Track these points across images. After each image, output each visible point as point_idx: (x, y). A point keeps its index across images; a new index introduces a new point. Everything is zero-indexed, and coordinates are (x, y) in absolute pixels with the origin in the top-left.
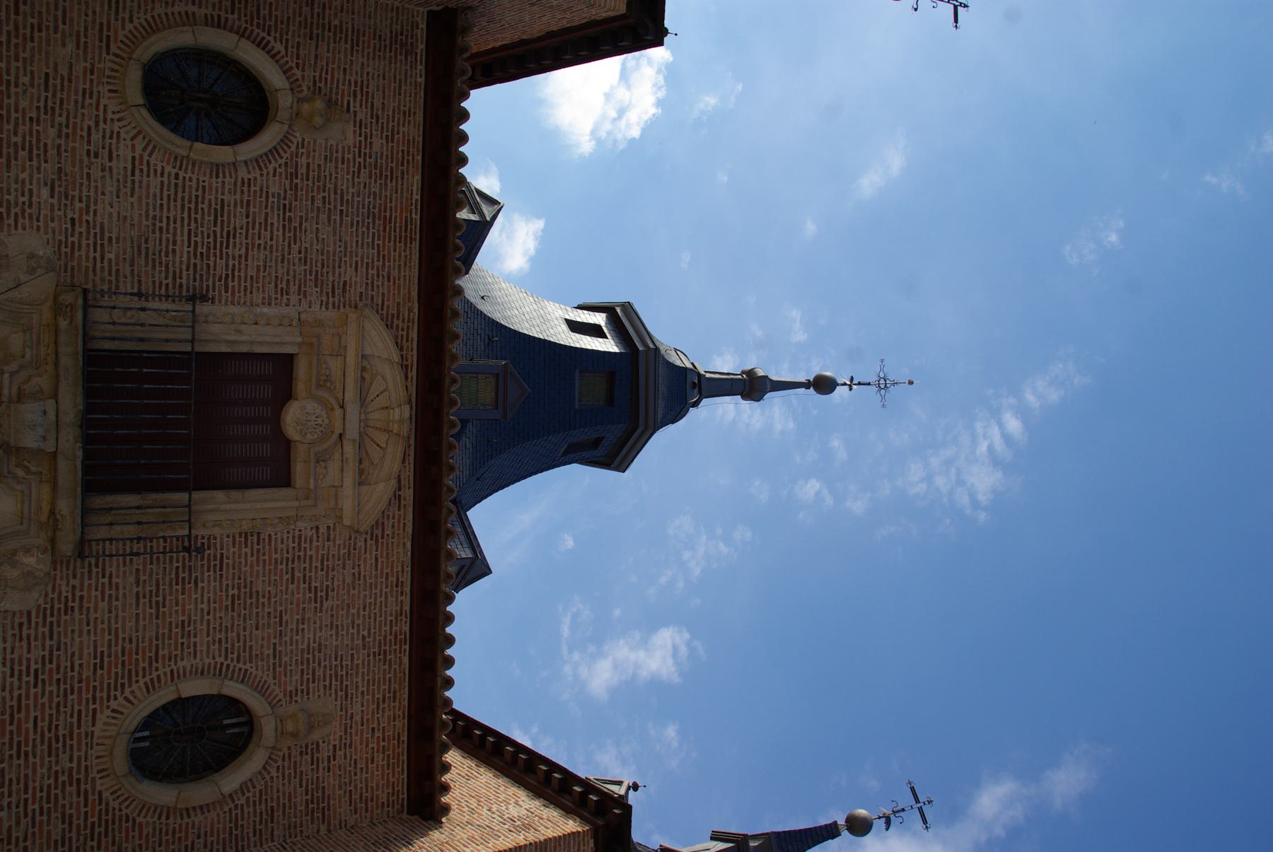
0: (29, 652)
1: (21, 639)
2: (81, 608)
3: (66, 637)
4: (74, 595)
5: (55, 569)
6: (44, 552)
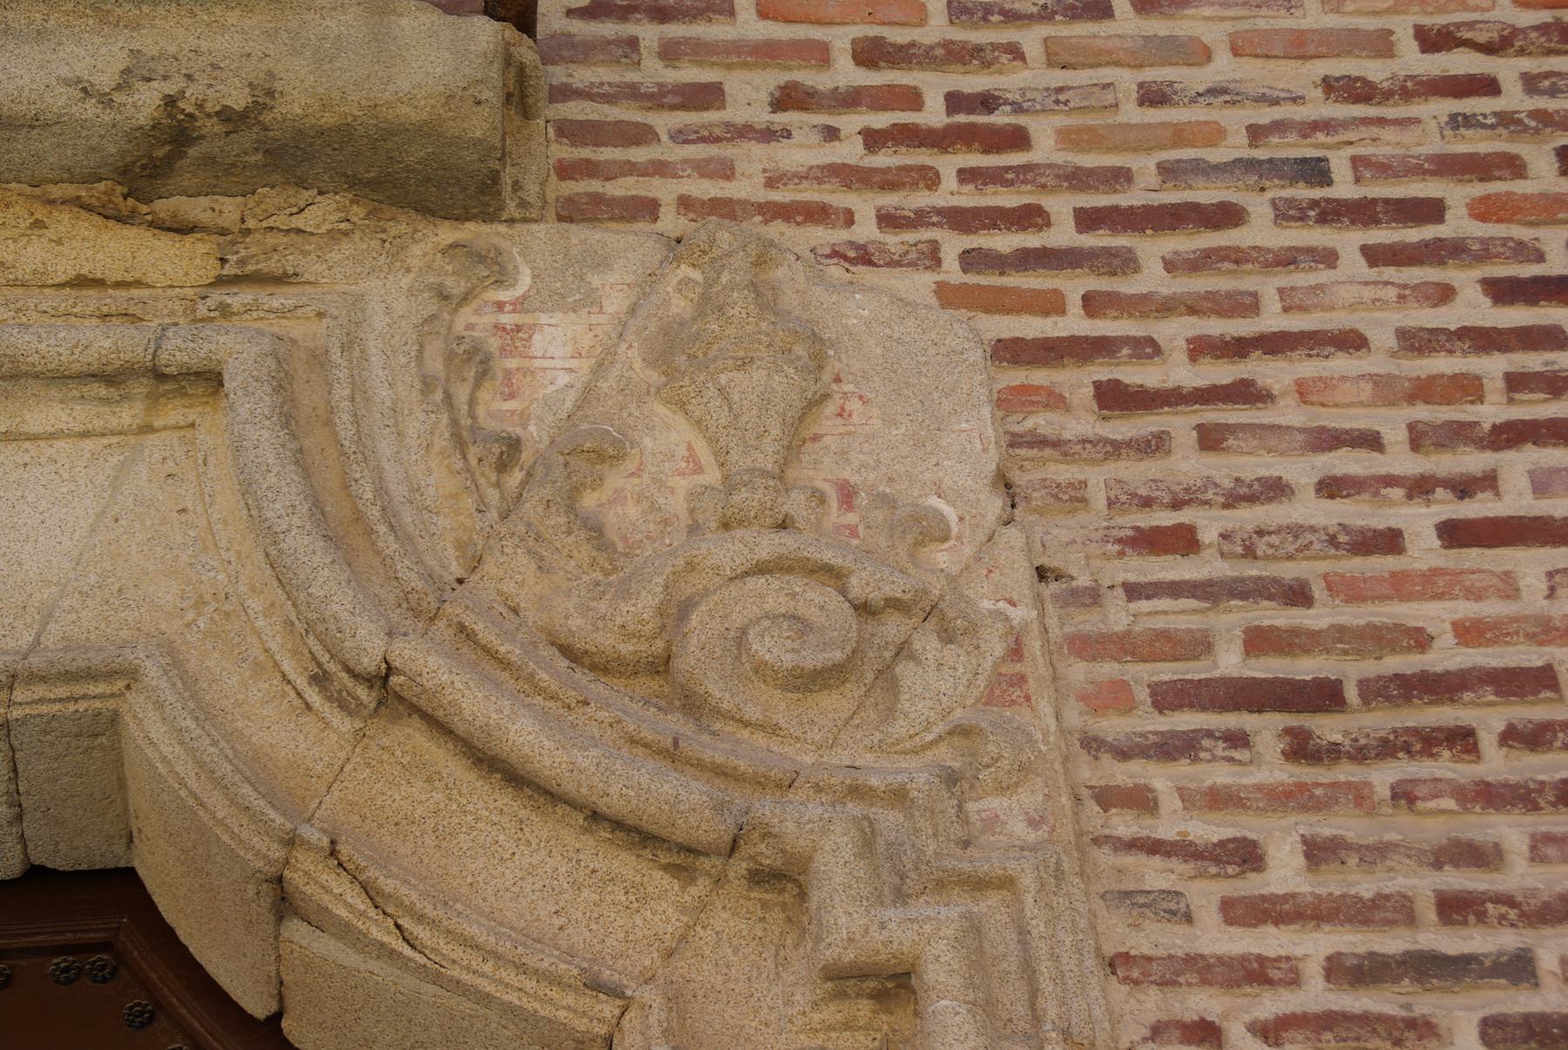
0: (1352, 342)
1: (1245, 393)
2: (956, 55)
3: (1215, 135)
4: (851, 99)
5: (648, 209)
6: (498, 270)
